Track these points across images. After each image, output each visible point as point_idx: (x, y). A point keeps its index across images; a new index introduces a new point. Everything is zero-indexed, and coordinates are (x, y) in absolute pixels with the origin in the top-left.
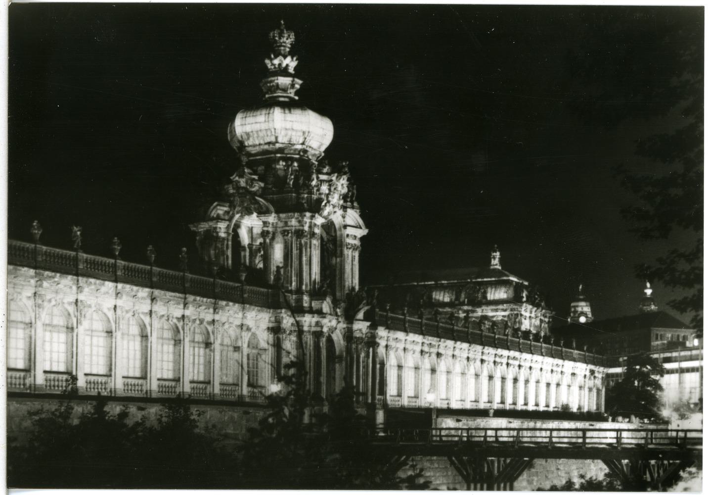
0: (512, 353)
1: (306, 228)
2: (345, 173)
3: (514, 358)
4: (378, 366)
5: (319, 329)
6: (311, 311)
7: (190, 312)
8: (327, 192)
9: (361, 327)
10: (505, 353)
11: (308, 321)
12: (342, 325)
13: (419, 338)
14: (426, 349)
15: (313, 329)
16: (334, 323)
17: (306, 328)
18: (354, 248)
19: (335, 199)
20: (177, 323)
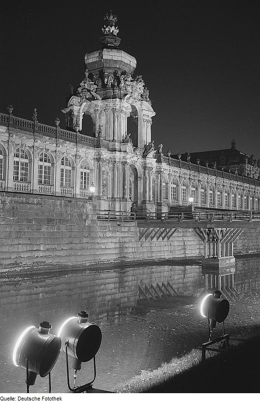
0: (239, 183)
1: (118, 107)
2: (140, 81)
3: (240, 186)
4: (164, 184)
5: (124, 160)
6: (120, 151)
7: (39, 143)
8: (131, 91)
9: (151, 161)
10: (236, 183)
11: (118, 155)
12: (141, 160)
13: (188, 172)
14: (192, 177)
15: (121, 160)
16: (135, 158)
17: (117, 160)
18: (148, 121)
19: (136, 95)
20: (29, 149)
